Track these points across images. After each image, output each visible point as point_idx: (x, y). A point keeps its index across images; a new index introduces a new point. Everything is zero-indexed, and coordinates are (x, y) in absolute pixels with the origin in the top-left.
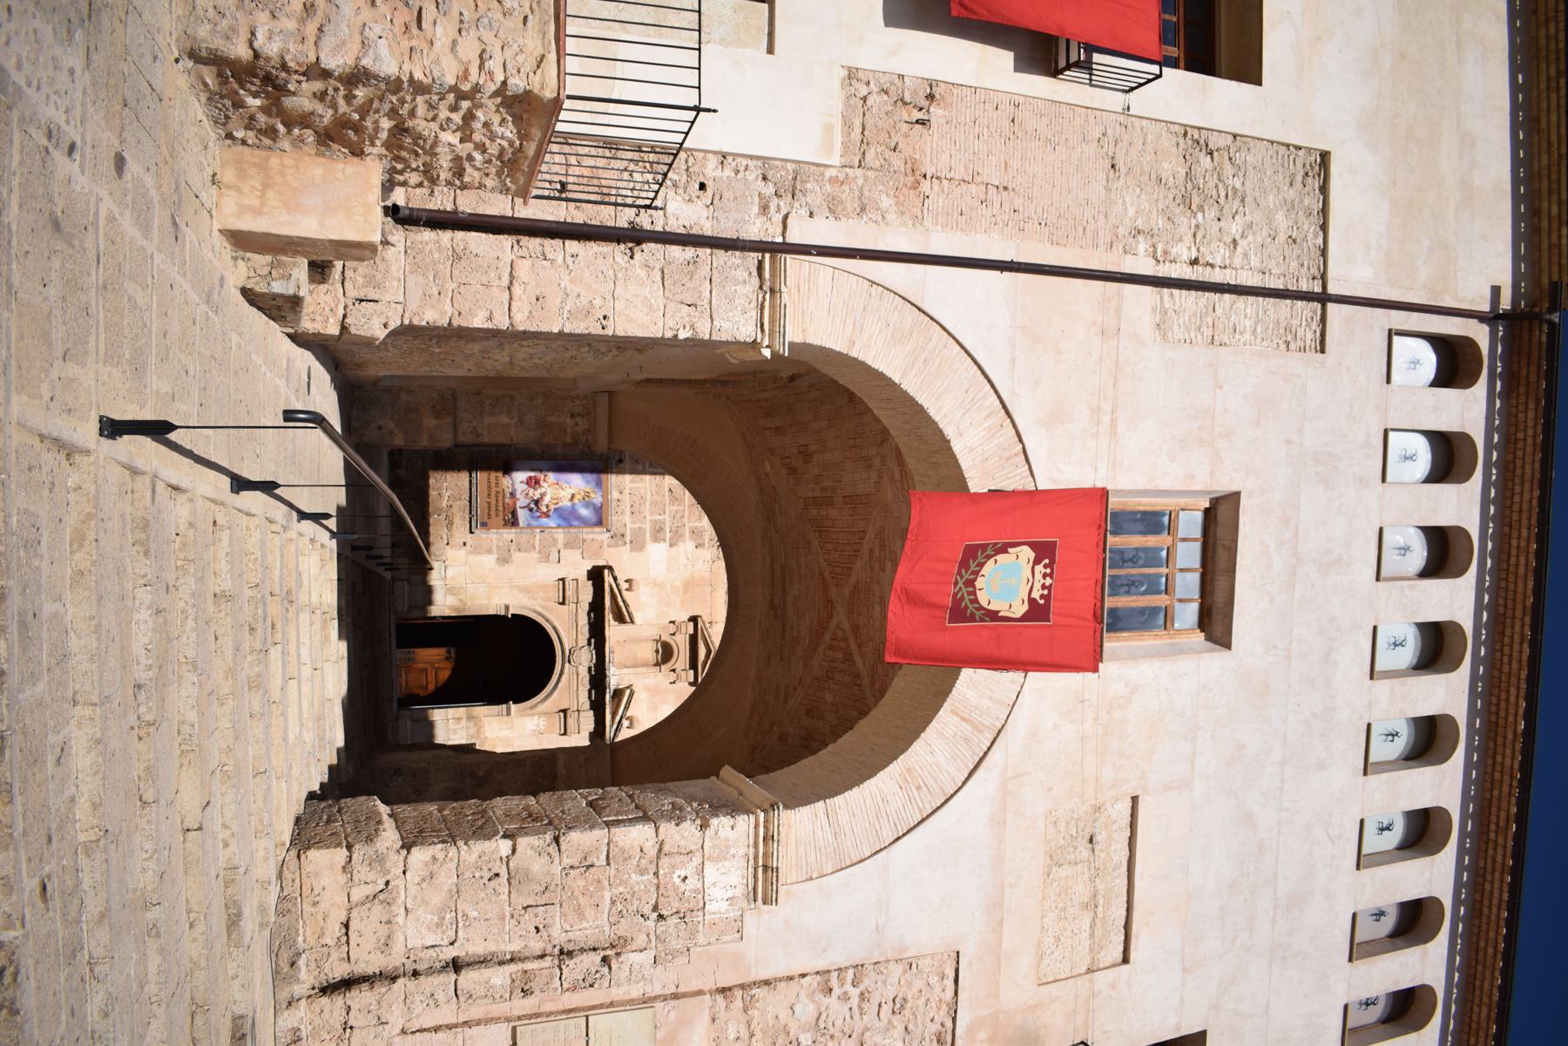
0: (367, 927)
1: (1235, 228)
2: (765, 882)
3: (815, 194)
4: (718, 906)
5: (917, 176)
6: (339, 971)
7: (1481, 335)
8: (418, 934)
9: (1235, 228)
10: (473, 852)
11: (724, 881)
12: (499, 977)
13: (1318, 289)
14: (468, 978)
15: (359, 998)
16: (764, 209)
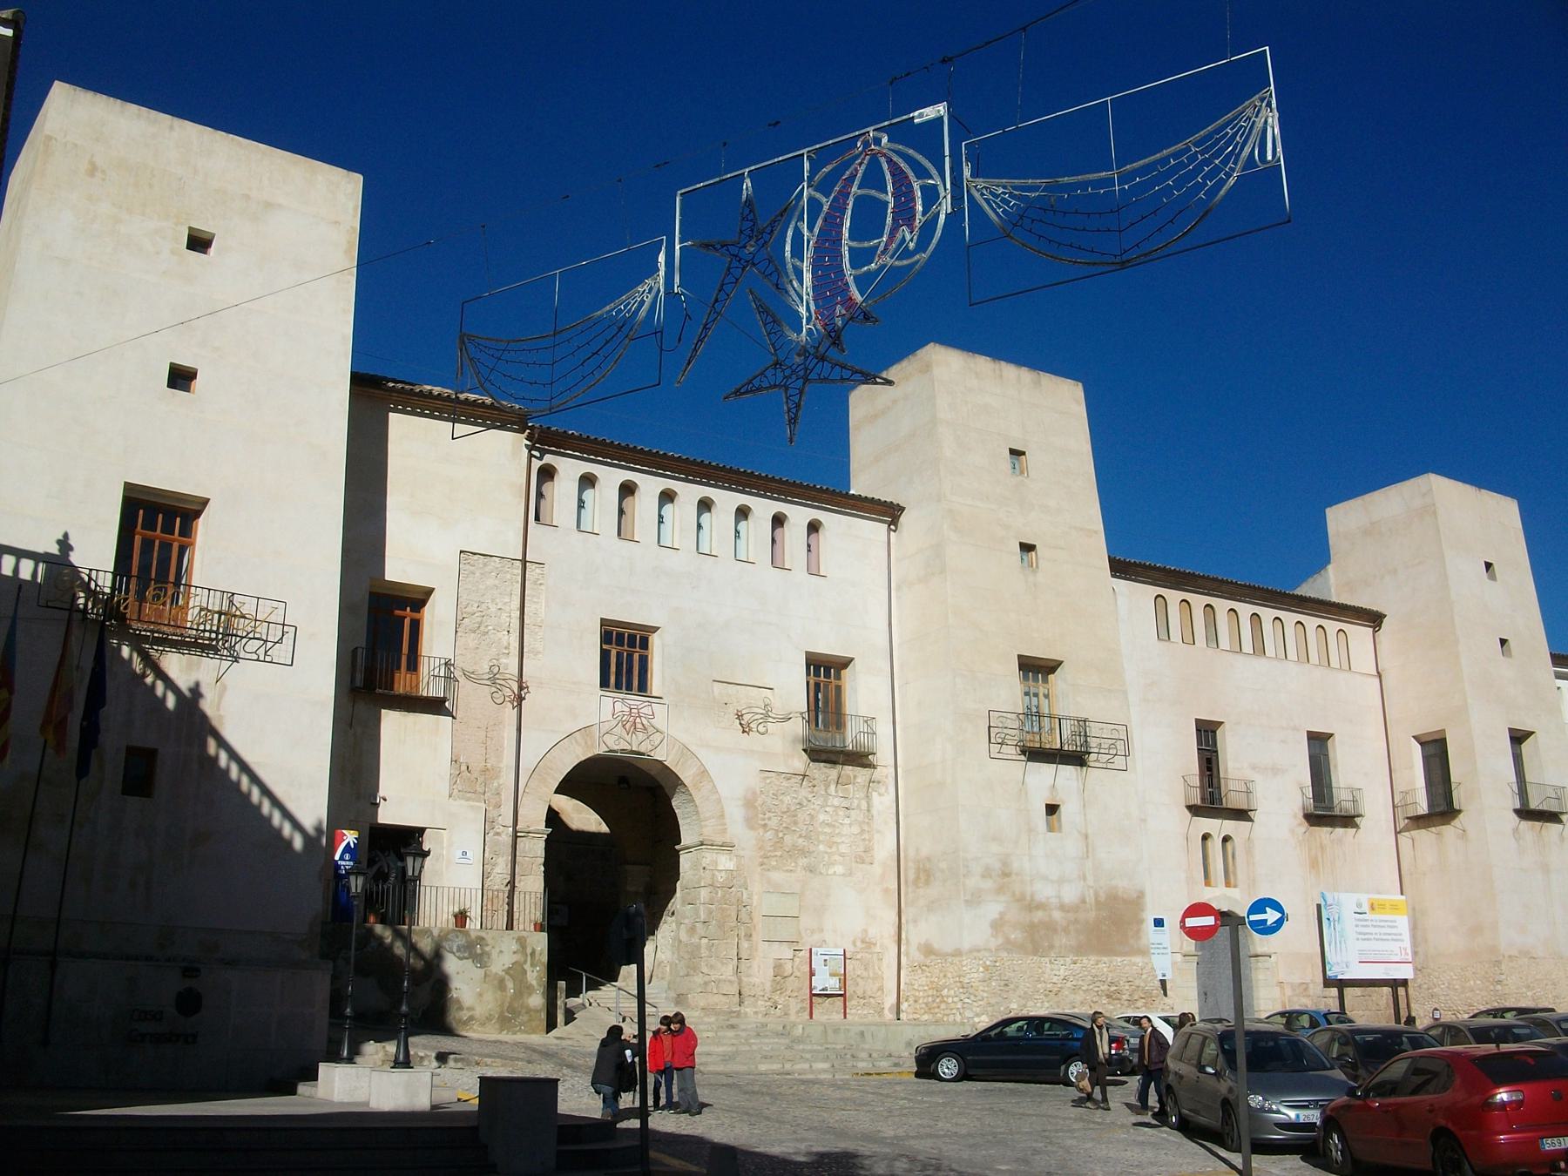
0: (726, 988)
1: (493, 608)
2: (727, 847)
3: (492, 814)
4: (731, 865)
5: (485, 771)
6: (737, 998)
7: (536, 464)
8: (728, 971)
9: (493, 608)
10: (704, 952)
11: (725, 862)
12: (745, 944)
13: (519, 564)
14: (744, 955)
15: (745, 991)
16: (498, 834)
